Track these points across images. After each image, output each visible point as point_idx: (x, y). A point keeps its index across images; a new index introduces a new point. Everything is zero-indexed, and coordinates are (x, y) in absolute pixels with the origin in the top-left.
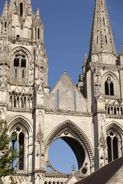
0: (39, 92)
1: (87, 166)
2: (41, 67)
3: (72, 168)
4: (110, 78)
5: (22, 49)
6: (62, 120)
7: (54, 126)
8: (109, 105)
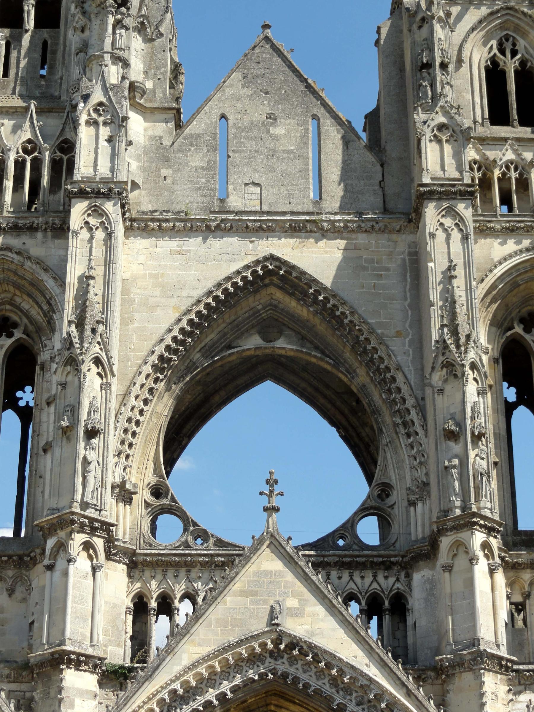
0: (94, 115)
1: (390, 501)
3: (261, 493)
4: (514, 45)
6: (234, 260)
7: (184, 294)
8: (508, 168)
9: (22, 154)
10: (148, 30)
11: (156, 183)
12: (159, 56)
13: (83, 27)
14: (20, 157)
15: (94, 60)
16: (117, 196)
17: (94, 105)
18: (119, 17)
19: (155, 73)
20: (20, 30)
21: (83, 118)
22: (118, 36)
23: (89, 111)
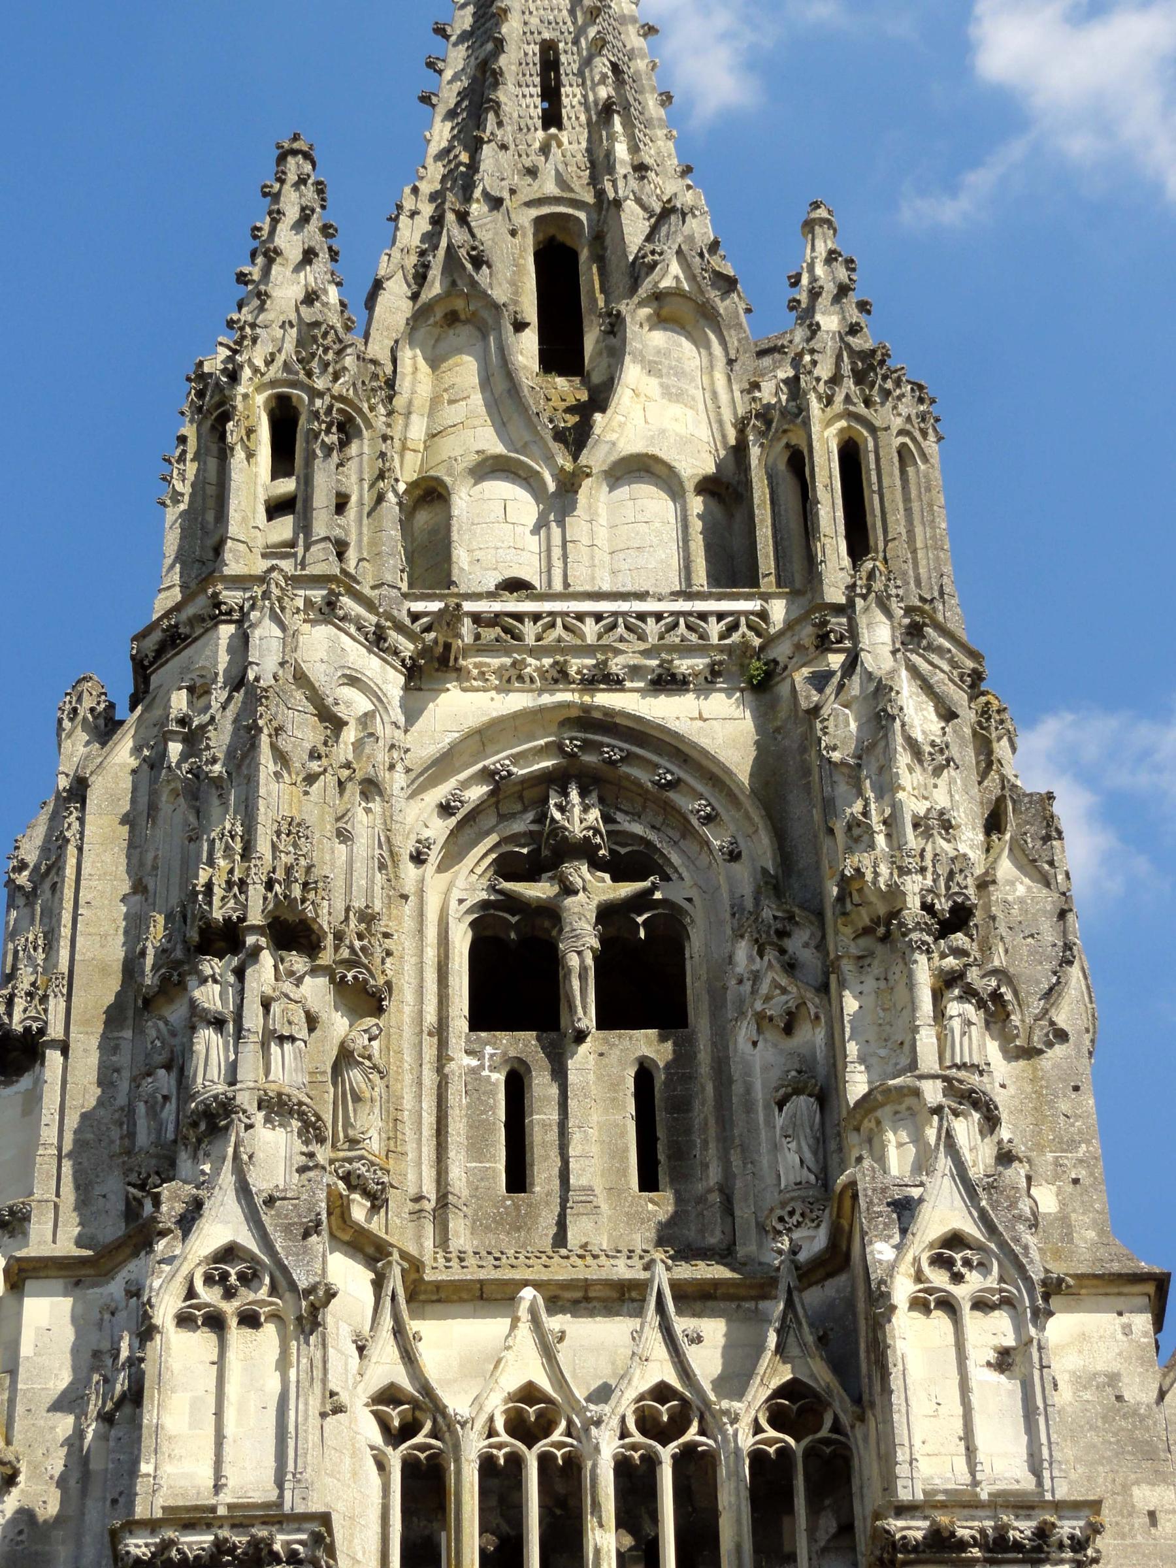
2: (943, 905)
5: (589, 758)
9: (638, 1438)
10: (1015, 1019)
11: (1123, 1536)
12: (1064, 1106)
13: (790, 1013)
14: (634, 1447)
15: (882, 1105)
16: (1069, 1555)
17: (931, 1246)
18: (951, 962)
19: (1057, 1163)
20: (553, 1035)
21: (902, 1290)
22: (956, 1024)
23: (916, 1261)
